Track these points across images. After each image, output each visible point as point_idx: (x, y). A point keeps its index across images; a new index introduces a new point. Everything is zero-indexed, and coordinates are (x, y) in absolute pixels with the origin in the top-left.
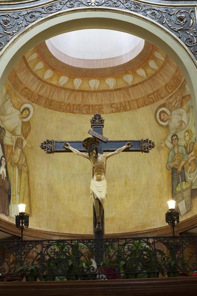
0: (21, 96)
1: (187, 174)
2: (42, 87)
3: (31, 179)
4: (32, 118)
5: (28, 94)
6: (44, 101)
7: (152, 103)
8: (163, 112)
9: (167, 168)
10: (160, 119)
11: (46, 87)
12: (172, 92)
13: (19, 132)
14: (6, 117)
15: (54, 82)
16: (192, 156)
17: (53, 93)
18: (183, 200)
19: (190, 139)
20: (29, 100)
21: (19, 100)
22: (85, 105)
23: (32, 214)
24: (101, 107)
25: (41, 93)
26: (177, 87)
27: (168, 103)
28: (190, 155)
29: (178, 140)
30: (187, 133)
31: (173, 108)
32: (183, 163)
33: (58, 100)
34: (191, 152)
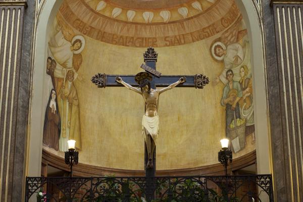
0: (73, 28)
1: (242, 111)
2: (95, 19)
3: (81, 111)
4: (83, 51)
6: (96, 33)
7: (207, 37)
8: (219, 46)
9: (221, 104)
10: (215, 53)
11: (98, 20)
12: (228, 26)
13: (70, 64)
14: (58, 49)
15: (107, 14)
16: (247, 92)
17: (106, 26)
18: (236, 137)
19: (245, 75)
20: (81, 32)
21: (70, 32)
22: (138, 38)
24: (155, 40)
25: (94, 25)
26: (233, 21)
28: (245, 91)
30: (242, 69)
31: (229, 43)
32: (238, 99)
33: (110, 32)
34: (247, 88)
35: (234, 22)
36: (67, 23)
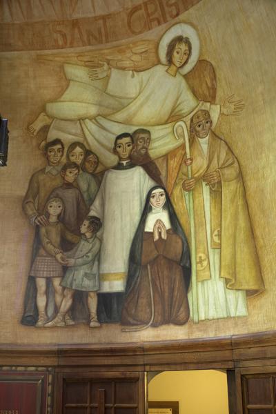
5: (148, 15)
13: (189, 103)
14: (133, 107)
20: (165, 21)
21: (140, 49)
23: (267, 287)
36: (115, 43)
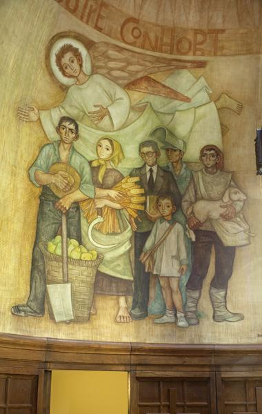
1: (87, 229)
9: (29, 175)
12: (133, 44)
26: (154, 49)
27: (102, 48)
28: (105, 192)
29: (77, 137)
31: (104, 71)
35: (157, 54)
